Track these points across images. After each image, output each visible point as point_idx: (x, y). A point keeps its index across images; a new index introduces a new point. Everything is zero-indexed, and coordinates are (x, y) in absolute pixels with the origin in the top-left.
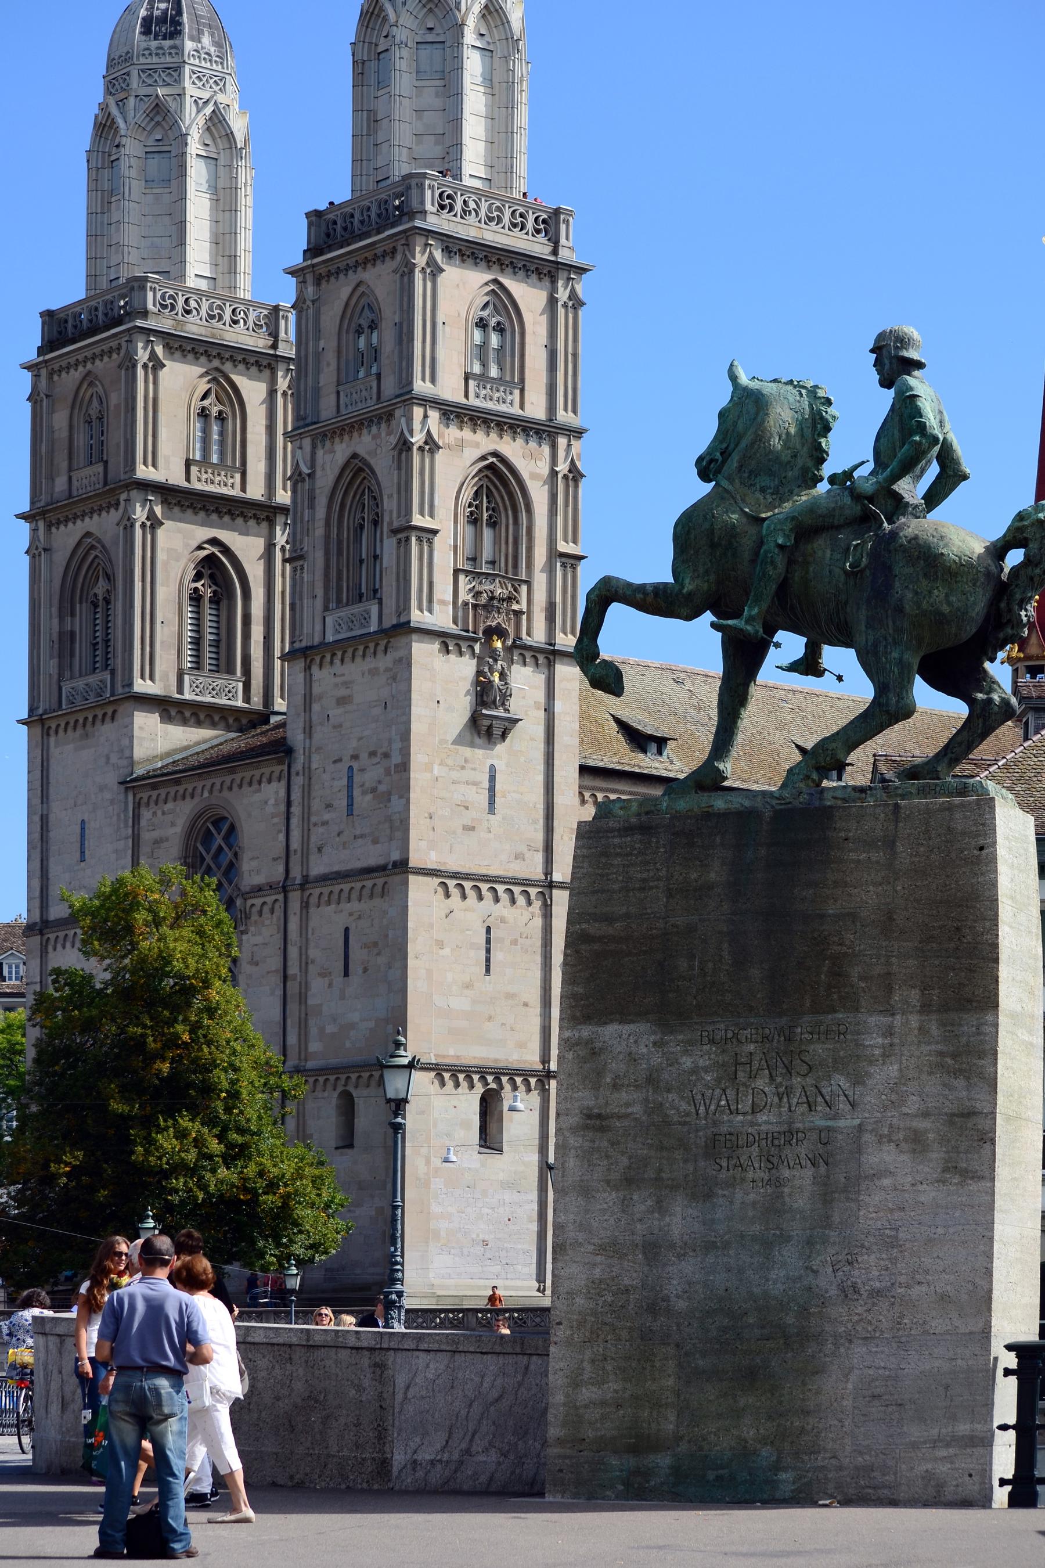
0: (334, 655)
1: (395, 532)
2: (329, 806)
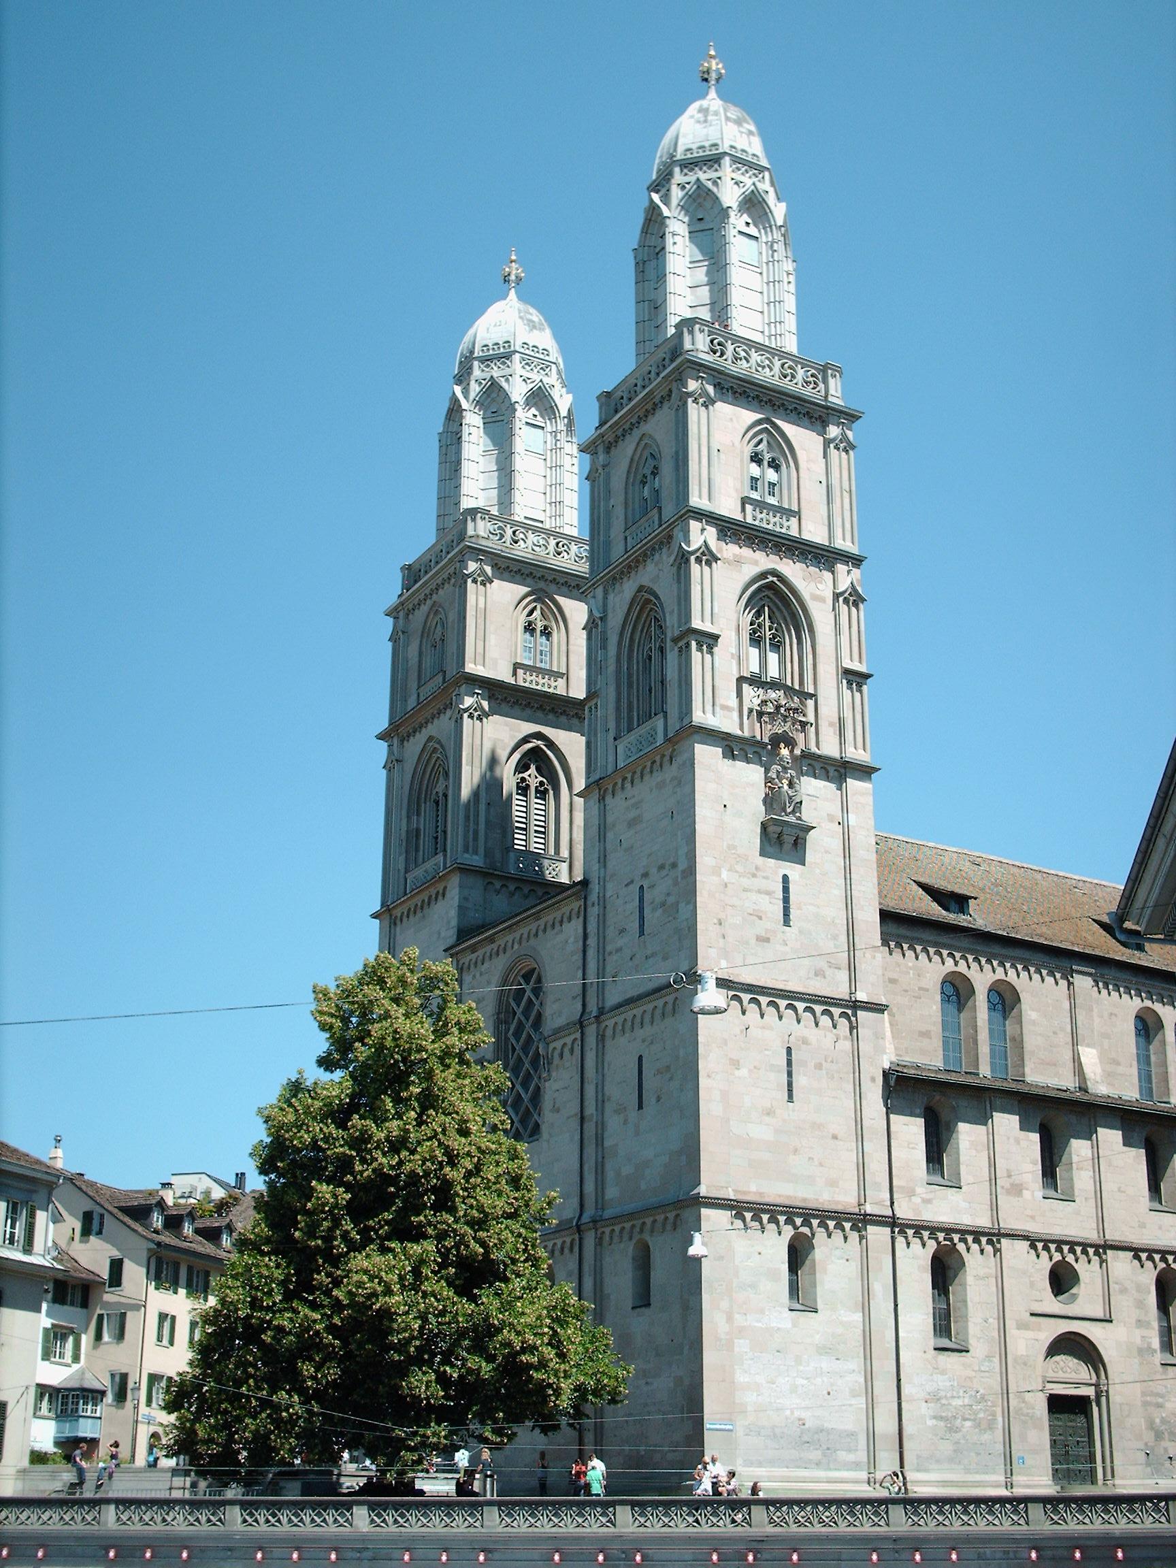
0: (624, 779)
1: (675, 640)
2: (622, 931)
